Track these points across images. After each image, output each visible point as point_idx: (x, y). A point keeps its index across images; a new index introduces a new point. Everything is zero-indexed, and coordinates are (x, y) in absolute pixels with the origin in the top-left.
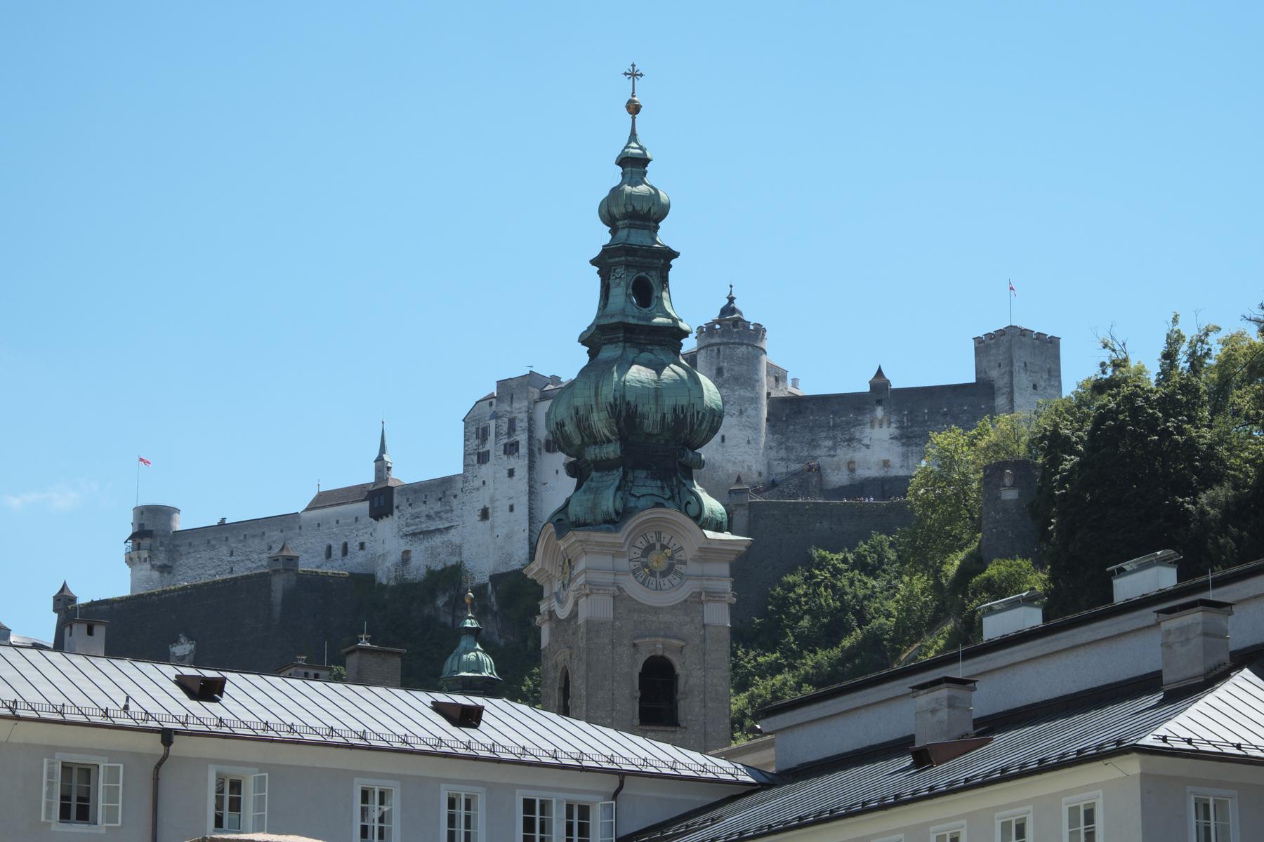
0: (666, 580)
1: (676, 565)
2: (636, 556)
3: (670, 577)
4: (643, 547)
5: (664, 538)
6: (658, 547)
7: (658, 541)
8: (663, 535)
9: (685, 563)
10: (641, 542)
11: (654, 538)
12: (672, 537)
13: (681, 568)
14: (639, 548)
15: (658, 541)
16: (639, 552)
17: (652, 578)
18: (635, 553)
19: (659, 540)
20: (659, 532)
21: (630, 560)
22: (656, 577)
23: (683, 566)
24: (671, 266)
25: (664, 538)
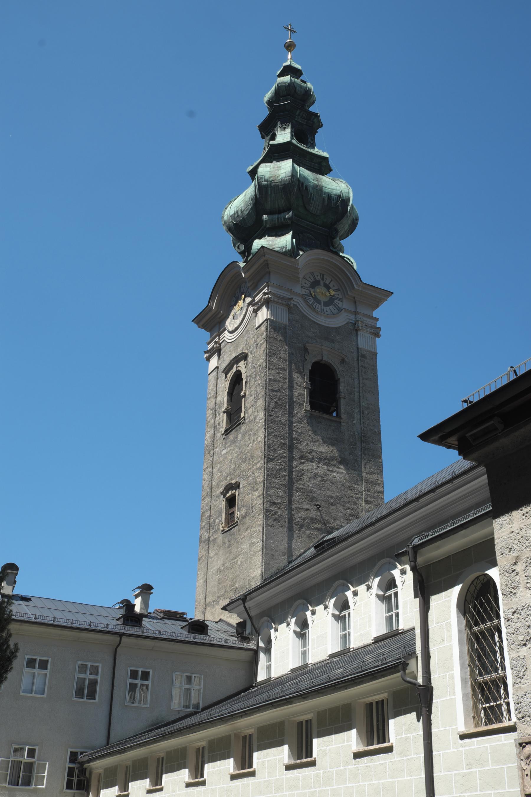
0: (328, 308)
1: (335, 301)
2: (306, 285)
3: (331, 307)
4: (312, 281)
5: (326, 279)
6: (322, 283)
7: (322, 280)
8: (325, 277)
9: (341, 300)
10: (310, 277)
11: (319, 277)
12: (332, 280)
13: (339, 303)
14: (308, 280)
15: (322, 280)
16: (309, 284)
17: (318, 305)
18: (305, 283)
19: (323, 279)
20: (322, 274)
21: (302, 287)
22: (321, 304)
23: (341, 303)
24: (317, 132)
25: (326, 279)
